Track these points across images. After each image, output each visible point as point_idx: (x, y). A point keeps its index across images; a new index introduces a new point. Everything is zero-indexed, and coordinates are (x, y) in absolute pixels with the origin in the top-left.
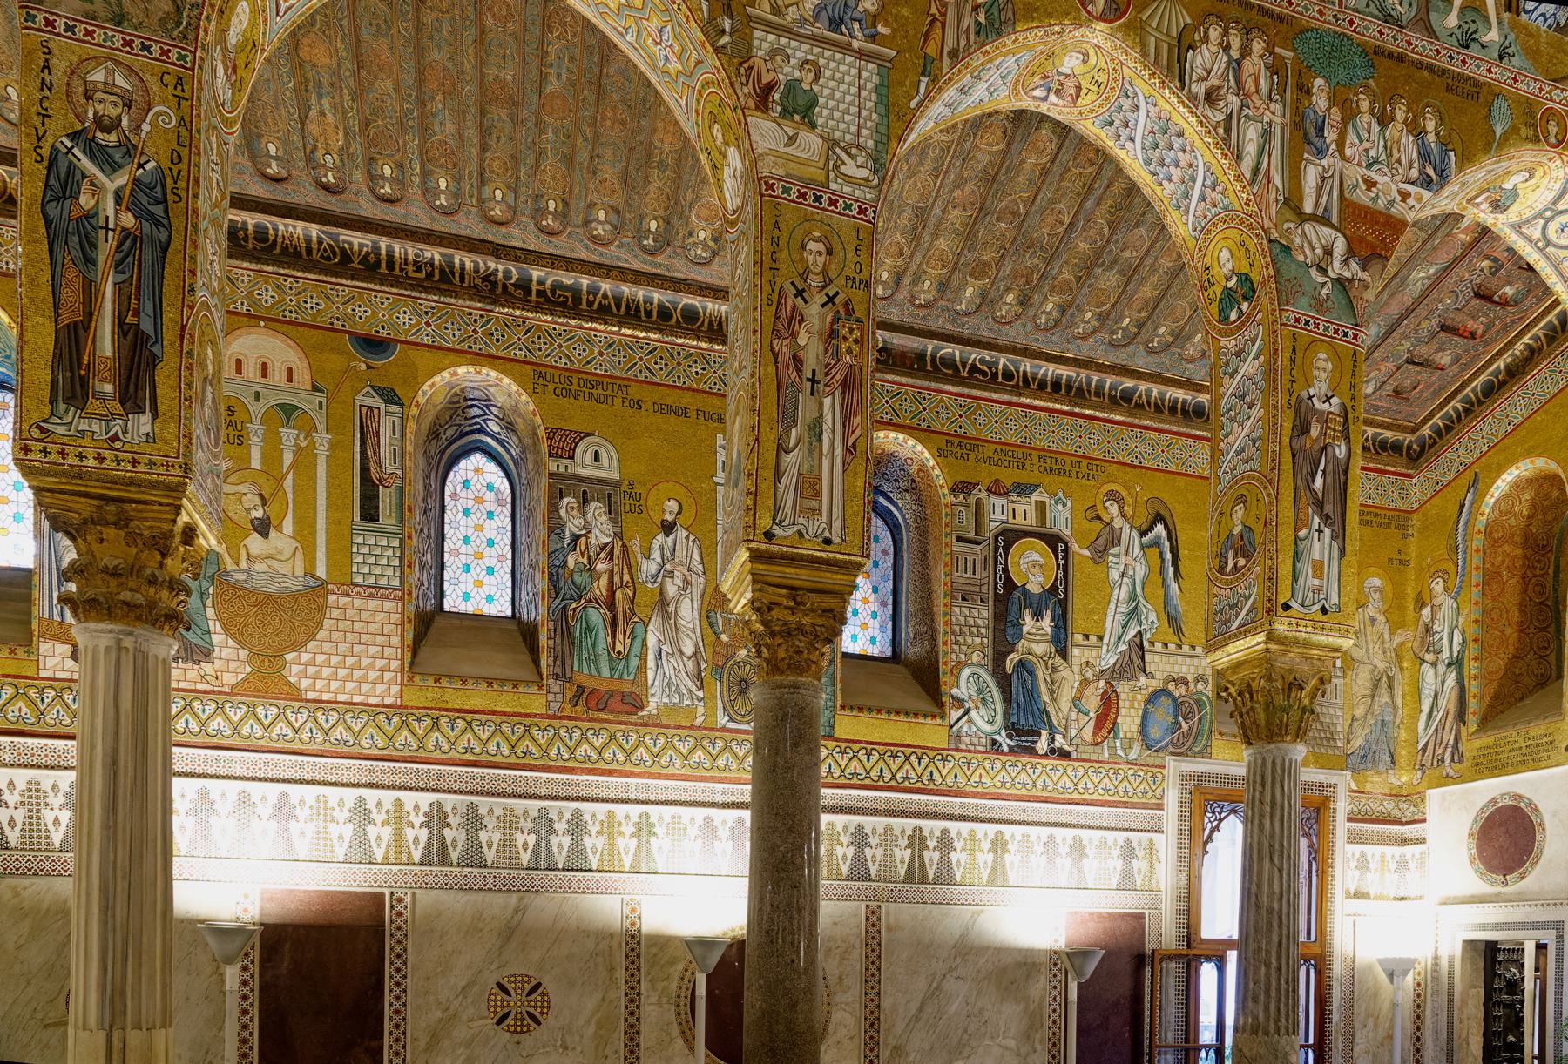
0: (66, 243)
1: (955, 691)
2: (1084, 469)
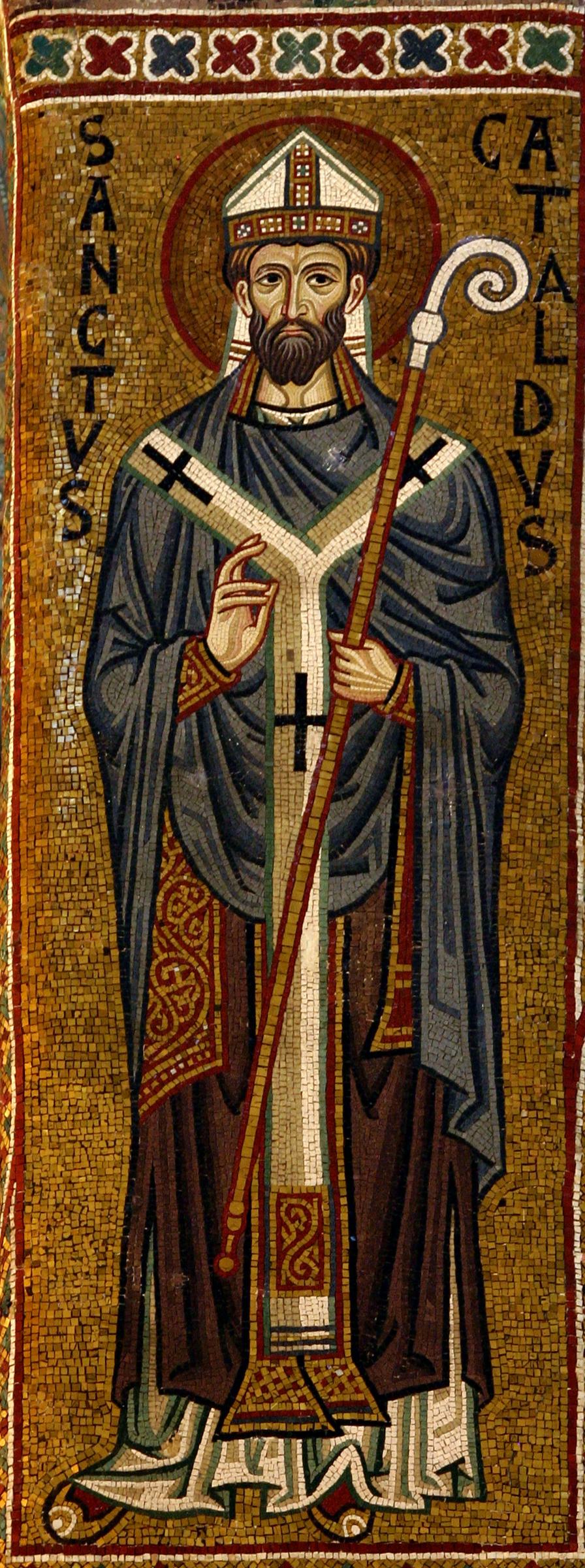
0: (167, 802)
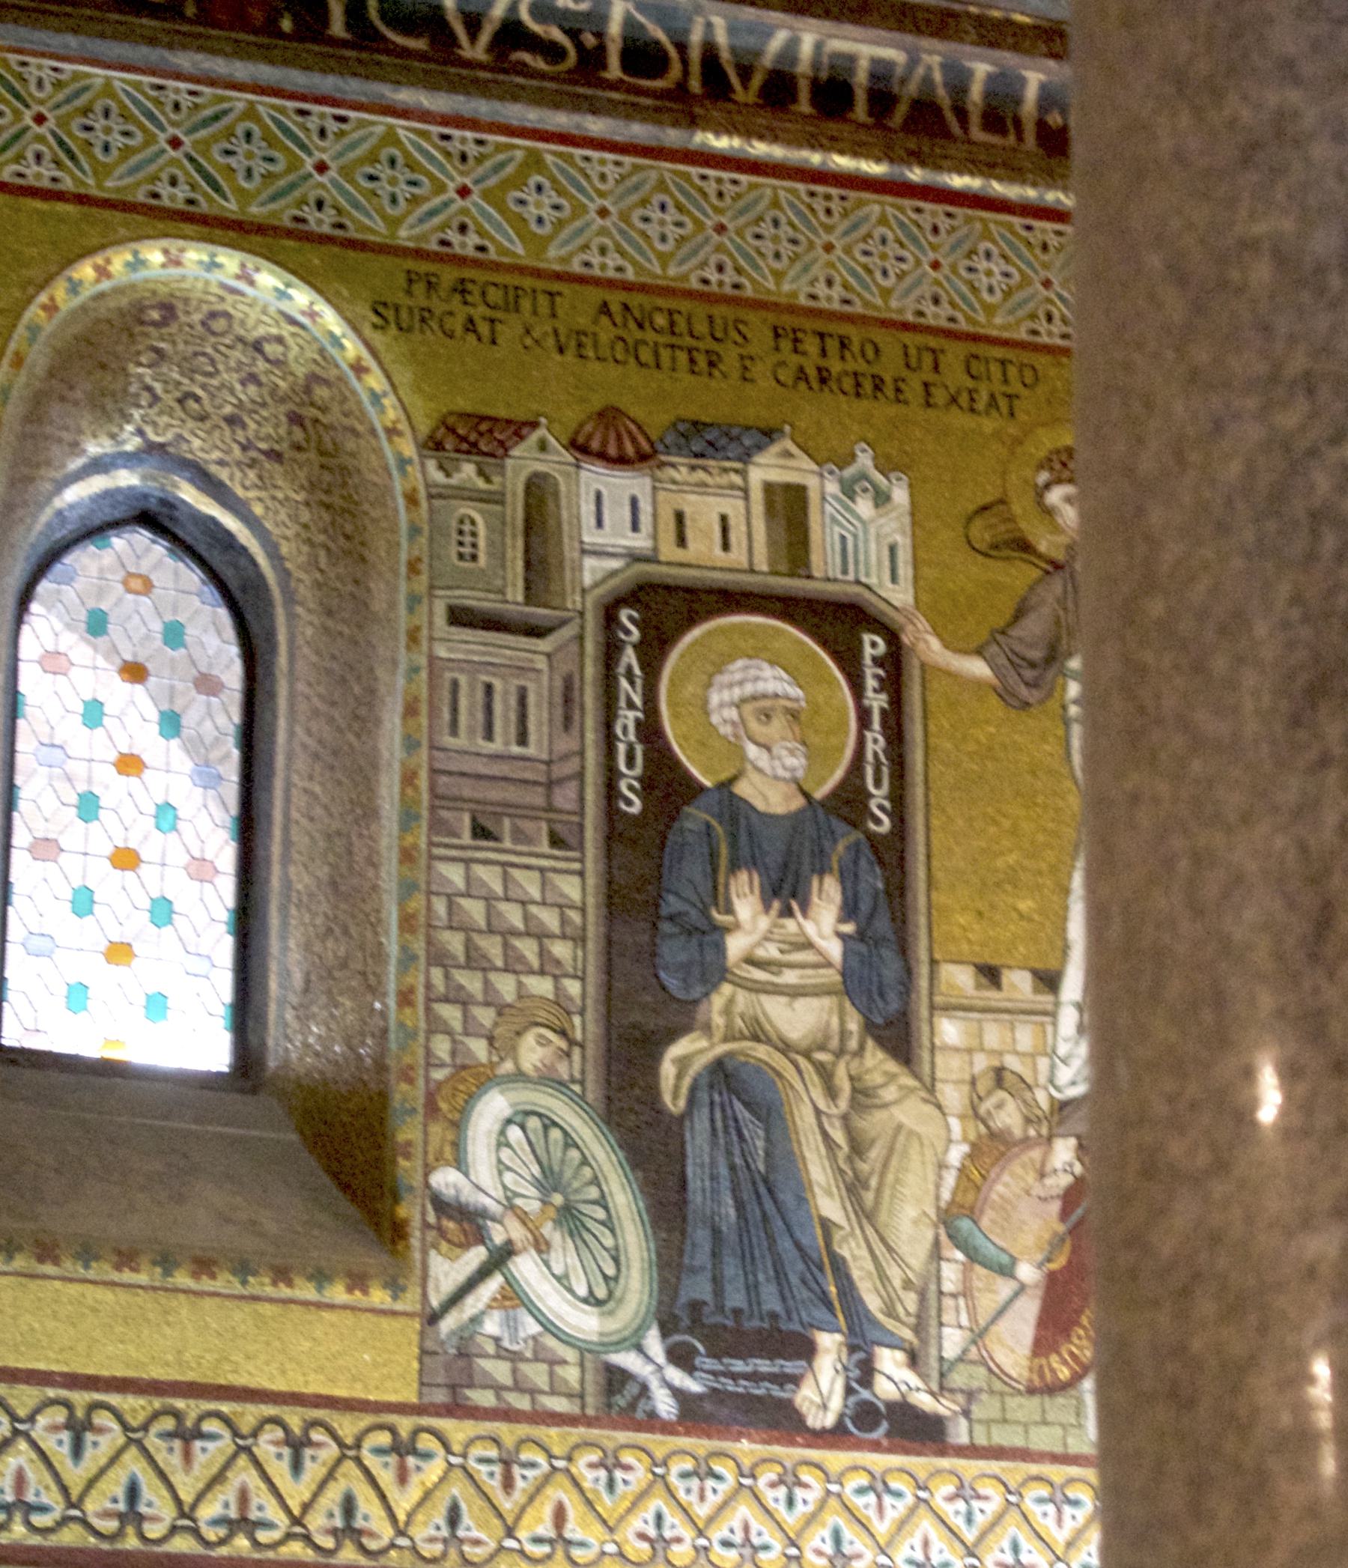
1: (446, 1180)
2: (954, 375)
